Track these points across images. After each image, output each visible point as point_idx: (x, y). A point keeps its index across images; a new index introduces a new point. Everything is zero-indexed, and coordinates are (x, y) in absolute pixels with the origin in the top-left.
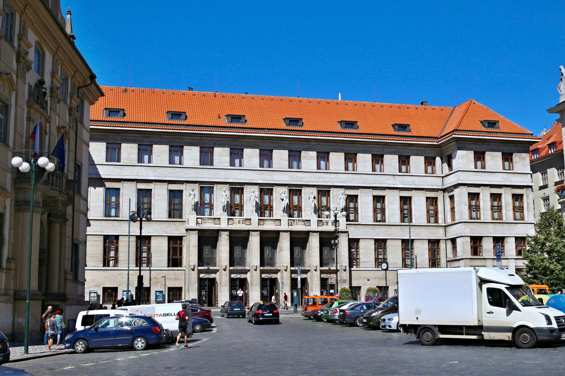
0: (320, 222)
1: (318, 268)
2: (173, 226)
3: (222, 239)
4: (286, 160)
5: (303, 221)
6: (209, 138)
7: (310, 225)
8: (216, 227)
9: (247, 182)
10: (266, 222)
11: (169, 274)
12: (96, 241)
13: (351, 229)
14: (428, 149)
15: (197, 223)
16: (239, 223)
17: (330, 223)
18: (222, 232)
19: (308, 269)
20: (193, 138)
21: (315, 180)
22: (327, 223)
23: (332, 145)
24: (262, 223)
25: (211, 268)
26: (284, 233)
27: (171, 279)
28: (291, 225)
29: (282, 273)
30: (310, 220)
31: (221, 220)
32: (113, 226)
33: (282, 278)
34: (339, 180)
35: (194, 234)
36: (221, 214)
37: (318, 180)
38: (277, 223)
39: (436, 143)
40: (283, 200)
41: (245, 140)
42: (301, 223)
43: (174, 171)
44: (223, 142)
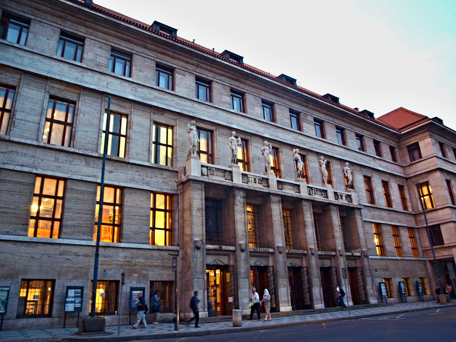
2: (159, 176)
3: (238, 203)
6: (208, 67)
9: (253, 132)
10: (286, 187)
11: (152, 257)
12: (20, 183)
14: (391, 138)
15: (202, 175)
16: (255, 182)
17: (344, 198)
18: (237, 192)
19: (333, 253)
20: (189, 60)
21: (316, 147)
23: (326, 114)
25: (224, 247)
27: (156, 266)
31: (234, 175)
32: (57, 160)
34: (335, 152)
35: (198, 189)
37: (319, 148)
39: (399, 133)
41: (248, 82)
42: (319, 193)
43: (161, 96)
44: (223, 78)
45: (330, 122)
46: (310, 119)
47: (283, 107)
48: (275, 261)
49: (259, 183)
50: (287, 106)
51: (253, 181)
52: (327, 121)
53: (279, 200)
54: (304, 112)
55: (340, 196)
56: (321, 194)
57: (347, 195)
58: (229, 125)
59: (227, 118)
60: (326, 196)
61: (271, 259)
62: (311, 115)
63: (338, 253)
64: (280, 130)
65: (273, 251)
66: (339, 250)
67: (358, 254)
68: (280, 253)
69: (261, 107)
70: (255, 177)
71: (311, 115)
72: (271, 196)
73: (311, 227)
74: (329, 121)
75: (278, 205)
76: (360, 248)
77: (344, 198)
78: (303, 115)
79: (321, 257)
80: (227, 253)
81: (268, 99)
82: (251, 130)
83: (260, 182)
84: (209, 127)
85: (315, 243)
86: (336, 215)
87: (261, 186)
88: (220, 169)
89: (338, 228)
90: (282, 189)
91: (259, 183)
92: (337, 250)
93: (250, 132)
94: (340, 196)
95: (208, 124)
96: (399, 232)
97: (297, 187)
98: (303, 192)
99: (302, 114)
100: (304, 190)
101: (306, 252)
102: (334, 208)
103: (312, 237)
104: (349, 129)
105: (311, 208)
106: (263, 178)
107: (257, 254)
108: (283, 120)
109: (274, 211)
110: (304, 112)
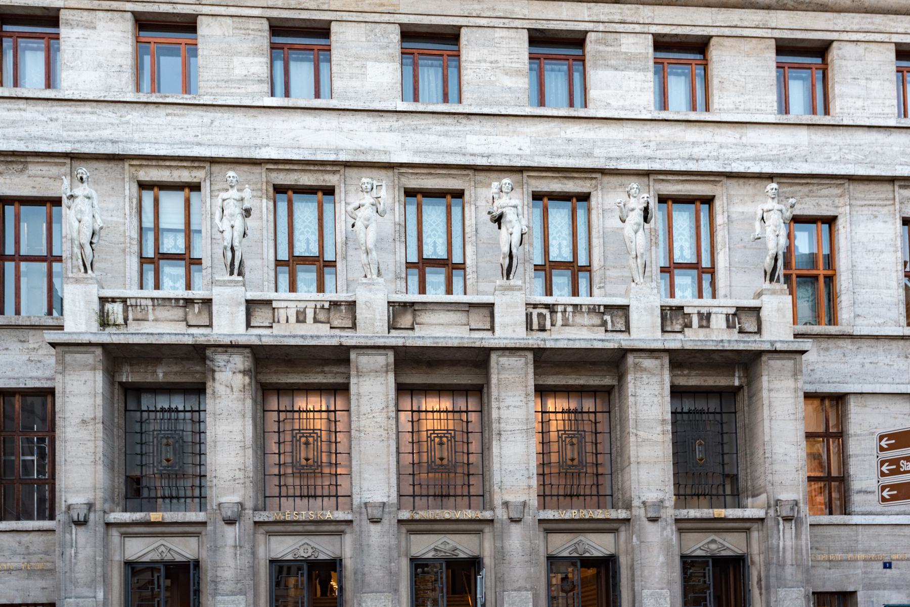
0: (672, 315)
1: (669, 513)
4: (518, 72)
5: (594, 310)
7: (628, 330)
8: (198, 335)
9: (343, 157)
10: (425, 318)
13: (814, 355)
17: (718, 322)
19: (622, 514)
22: (705, 319)
24: (406, 320)
26: (503, 360)
28: (542, 329)
29: (501, 536)
30: (625, 308)
33: (501, 555)
36: (224, 284)
38: (478, 319)
42: (586, 319)
45: (746, 32)
46: (633, 50)
47: (499, 33)
48: (360, 548)
49: (316, 321)
50: (517, 23)
51: (293, 319)
52: (727, 32)
53: (387, 365)
54: (601, 27)
55: (695, 320)
56: (597, 320)
57: (738, 308)
58: (246, 154)
59: (248, 130)
60: (620, 325)
61: (348, 539)
62: (638, 28)
63: (639, 512)
64: (475, 121)
65: (349, 517)
66: (644, 503)
67: (760, 513)
68: (375, 521)
69: (392, 58)
70: (302, 305)
71: (638, 28)
72: (353, 355)
73: (519, 437)
74: (738, 32)
75: (381, 379)
76: (765, 491)
77: (718, 322)
78: (597, 42)
79: (549, 527)
80: (193, 529)
81: (426, 20)
82: (337, 151)
83: (322, 316)
84: (184, 176)
85: (529, 487)
86: (657, 387)
87: (324, 329)
88: (170, 299)
89: (659, 429)
90: (413, 329)
91: (316, 321)
92: (636, 503)
93: (332, 158)
94: (695, 320)
95: (178, 167)
96: (842, 418)
97: (486, 312)
98: (505, 326)
99: (591, 37)
100: (507, 320)
101: (487, 515)
102: (648, 363)
103: (523, 467)
104: (854, 37)
105: (531, 376)
106: (335, 304)
107: (299, 528)
108: (492, 83)
109: (364, 400)
110: (601, 27)
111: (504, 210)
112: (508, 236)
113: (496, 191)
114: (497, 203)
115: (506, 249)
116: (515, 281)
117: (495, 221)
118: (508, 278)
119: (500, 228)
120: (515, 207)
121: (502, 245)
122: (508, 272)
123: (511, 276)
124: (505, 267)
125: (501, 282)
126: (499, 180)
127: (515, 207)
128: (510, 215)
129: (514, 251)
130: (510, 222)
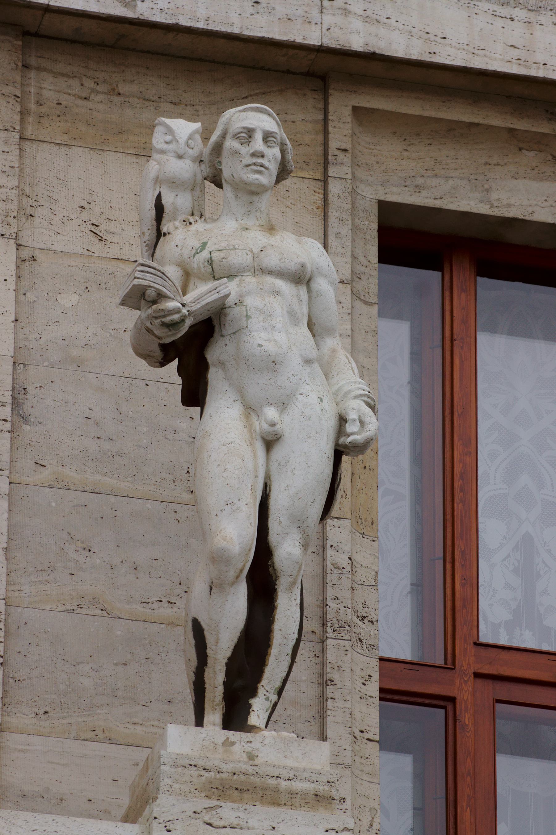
40: (191, 350)
111: (231, 288)
112: (245, 458)
113: (184, 169)
114: (182, 239)
115: (236, 534)
116: (271, 746)
117: (167, 353)
118: (235, 716)
119: (194, 394)
120: (301, 278)
121: (214, 495)
122: (235, 686)
123: (259, 708)
124: (223, 642)
125: (189, 742)
126: (206, 111)
127: (301, 278)
128: (268, 324)
129: (288, 550)
130: (273, 364)
